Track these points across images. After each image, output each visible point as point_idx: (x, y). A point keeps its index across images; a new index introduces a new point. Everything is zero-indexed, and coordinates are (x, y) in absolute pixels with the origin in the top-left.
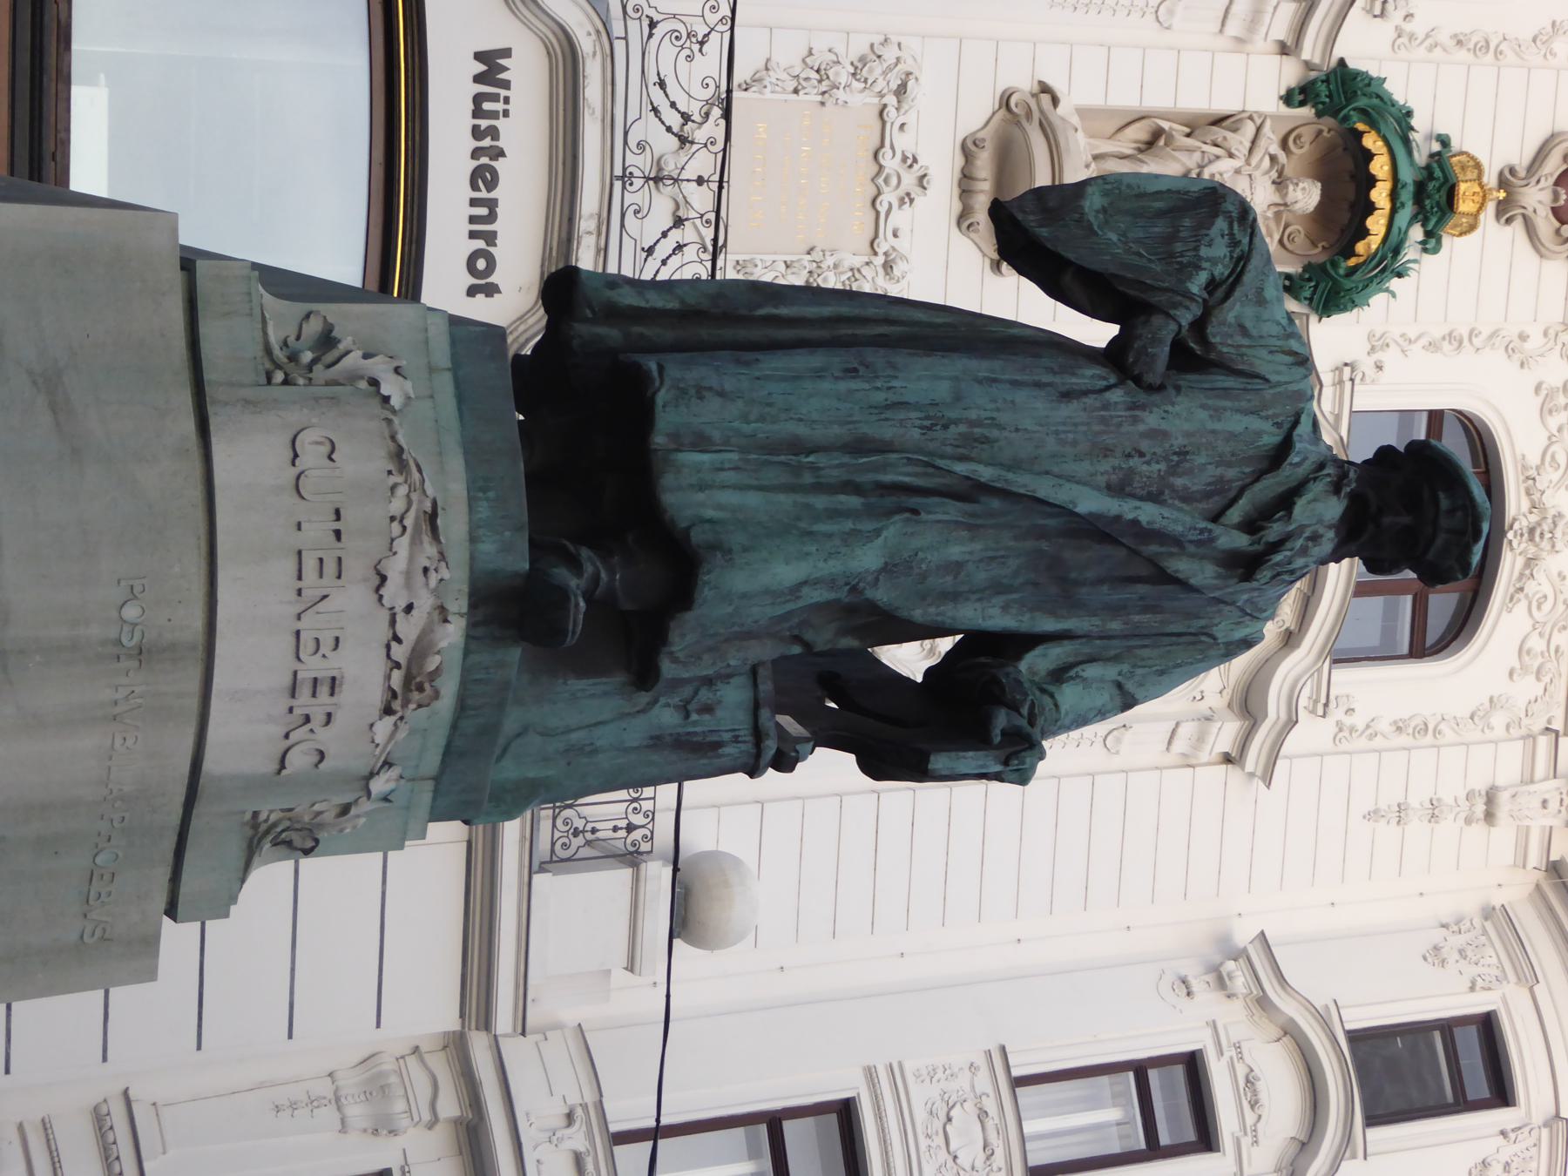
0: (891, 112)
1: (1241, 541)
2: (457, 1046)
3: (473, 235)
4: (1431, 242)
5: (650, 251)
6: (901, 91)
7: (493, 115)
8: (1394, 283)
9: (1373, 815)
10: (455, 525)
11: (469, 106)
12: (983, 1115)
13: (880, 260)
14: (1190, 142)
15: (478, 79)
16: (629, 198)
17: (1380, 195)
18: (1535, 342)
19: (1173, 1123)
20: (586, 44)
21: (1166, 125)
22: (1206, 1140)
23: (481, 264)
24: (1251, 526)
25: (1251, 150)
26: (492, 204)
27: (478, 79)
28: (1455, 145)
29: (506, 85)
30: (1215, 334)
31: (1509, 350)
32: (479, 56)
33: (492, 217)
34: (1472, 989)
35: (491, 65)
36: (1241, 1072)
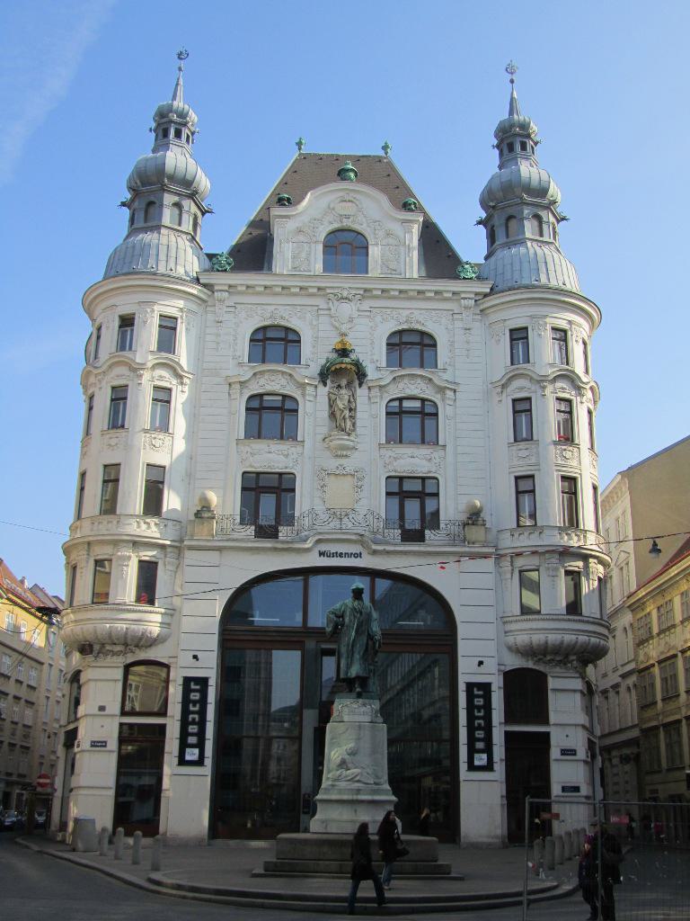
2: (499, 557)
9: (468, 356)
10: (352, 700)
12: (520, 450)
17: (343, 366)
22: (529, 399)
35: (322, 554)
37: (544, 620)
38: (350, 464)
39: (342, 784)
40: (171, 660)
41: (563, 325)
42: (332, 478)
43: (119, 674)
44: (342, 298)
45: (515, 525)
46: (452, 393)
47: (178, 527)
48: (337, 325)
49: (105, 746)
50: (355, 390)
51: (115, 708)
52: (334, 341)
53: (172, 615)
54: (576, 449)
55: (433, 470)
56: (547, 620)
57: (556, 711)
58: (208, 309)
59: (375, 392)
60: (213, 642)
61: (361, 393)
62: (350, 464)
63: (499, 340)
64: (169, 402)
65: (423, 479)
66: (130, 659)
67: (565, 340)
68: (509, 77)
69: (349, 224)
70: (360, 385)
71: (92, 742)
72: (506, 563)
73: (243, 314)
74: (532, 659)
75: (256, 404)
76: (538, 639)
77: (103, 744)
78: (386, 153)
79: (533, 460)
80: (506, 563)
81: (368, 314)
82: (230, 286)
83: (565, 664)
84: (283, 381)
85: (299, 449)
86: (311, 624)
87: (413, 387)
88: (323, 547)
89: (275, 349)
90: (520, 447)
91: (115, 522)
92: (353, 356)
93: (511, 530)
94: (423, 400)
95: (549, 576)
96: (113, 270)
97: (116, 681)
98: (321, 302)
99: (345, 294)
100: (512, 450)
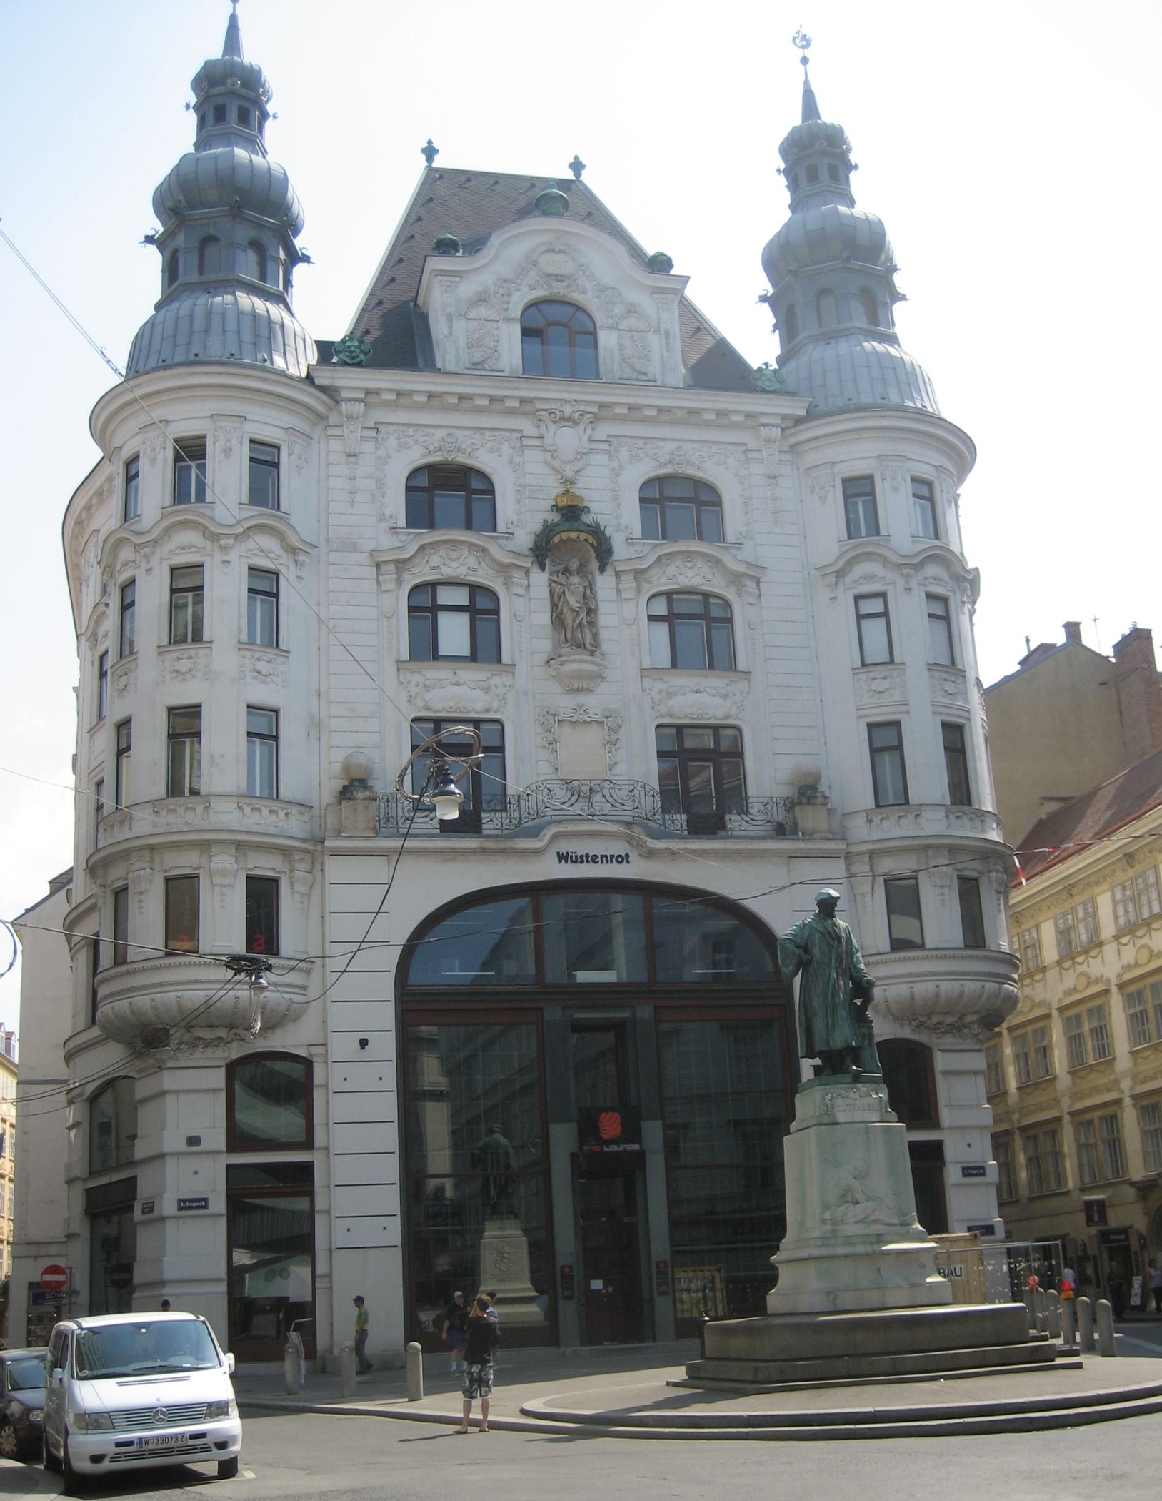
0: (560, 718)
1: (836, 942)
2: (848, 856)
3: (612, 862)
4: (586, 510)
5: (613, 806)
6: (555, 715)
7: (576, 856)
8: (602, 528)
11: (574, 865)
12: (874, 679)
13: (605, 720)
14: (559, 608)
15: (566, 862)
16: (598, 813)
18: (615, 464)
19: (875, 606)
20: (554, 829)
21: (554, 615)
22: (883, 595)
23: (620, 859)
24: (833, 939)
25: (561, 584)
26: (602, 856)
27: (566, 862)
28: (554, 503)
29: (567, 853)
30: (803, 944)
31: (619, 475)
32: (560, 862)
33: (606, 856)
34: (834, 487)
35: (562, 858)
36: (861, 581)
37: (932, 958)
38: (595, 703)
39: (850, 1229)
40: (314, 1050)
41: (927, 472)
42: (567, 729)
43: (218, 1079)
44: (562, 419)
45: (873, 806)
46: (753, 585)
47: (306, 817)
48: (556, 464)
49: (206, 1207)
50: (593, 577)
51: (216, 1138)
52: (551, 490)
53: (308, 972)
54: (960, 680)
55: (733, 712)
56: (937, 957)
57: (949, 1106)
58: (330, 431)
59: (628, 582)
60: (386, 1016)
61: (604, 582)
62: (595, 703)
63: (825, 497)
64: (276, 595)
65: (716, 729)
66: (236, 1052)
67: (931, 499)
68: (800, 53)
69: (562, 292)
70: (602, 569)
71: (180, 1201)
72: (862, 867)
73: (392, 442)
74: (910, 1024)
75: (424, 600)
76: (923, 989)
77: (202, 1203)
78: (578, 175)
79: (897, 697)
80: (862, 867)
81: (605, 446)
82: (368, 392)
83: (959, 1030)
84: (472, 561)
85: (507, 679)
86: (549, 978)
87: (690, 573)
88: (565, 846)
89: (448, 502)
90: (876, 675)
91: (199, 809)
92: (587, 519)
93: (867, 812)
94: (706, 596)
95: (935, 886)
96: (154, 357)
97: (214, 1091)
98: (528, 427)
99: (567, 410)
100: (860, 680)
